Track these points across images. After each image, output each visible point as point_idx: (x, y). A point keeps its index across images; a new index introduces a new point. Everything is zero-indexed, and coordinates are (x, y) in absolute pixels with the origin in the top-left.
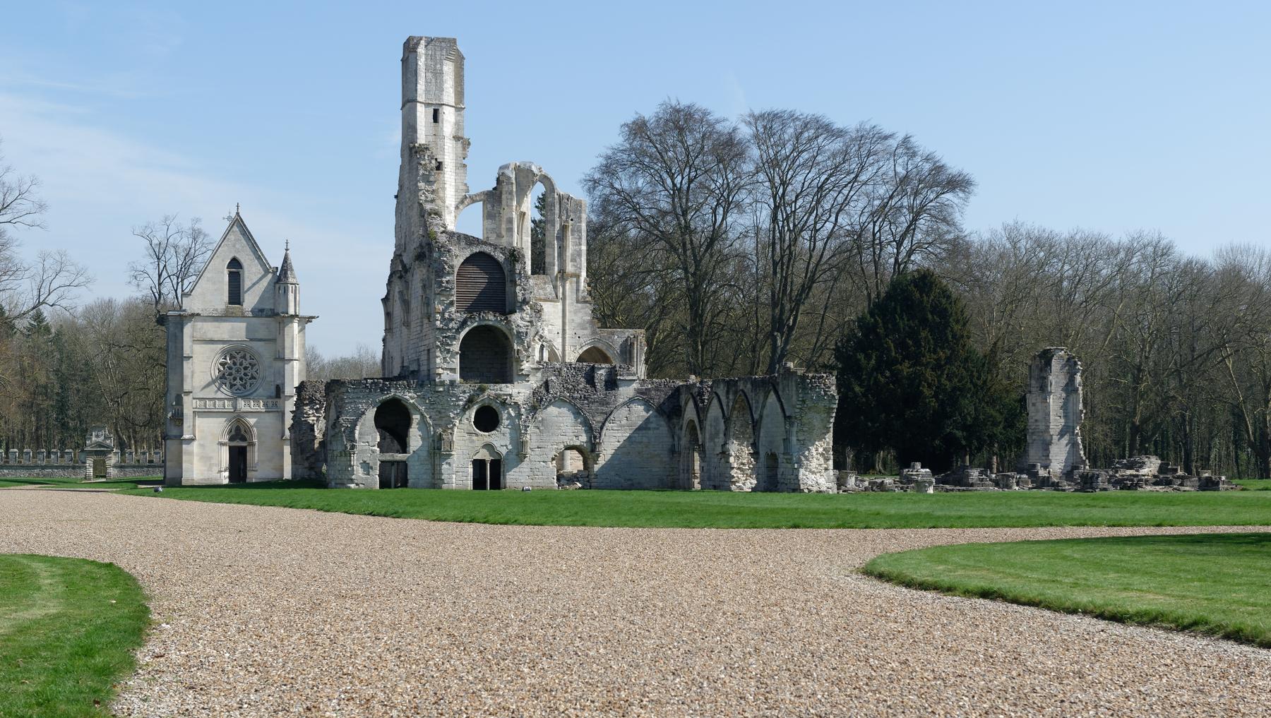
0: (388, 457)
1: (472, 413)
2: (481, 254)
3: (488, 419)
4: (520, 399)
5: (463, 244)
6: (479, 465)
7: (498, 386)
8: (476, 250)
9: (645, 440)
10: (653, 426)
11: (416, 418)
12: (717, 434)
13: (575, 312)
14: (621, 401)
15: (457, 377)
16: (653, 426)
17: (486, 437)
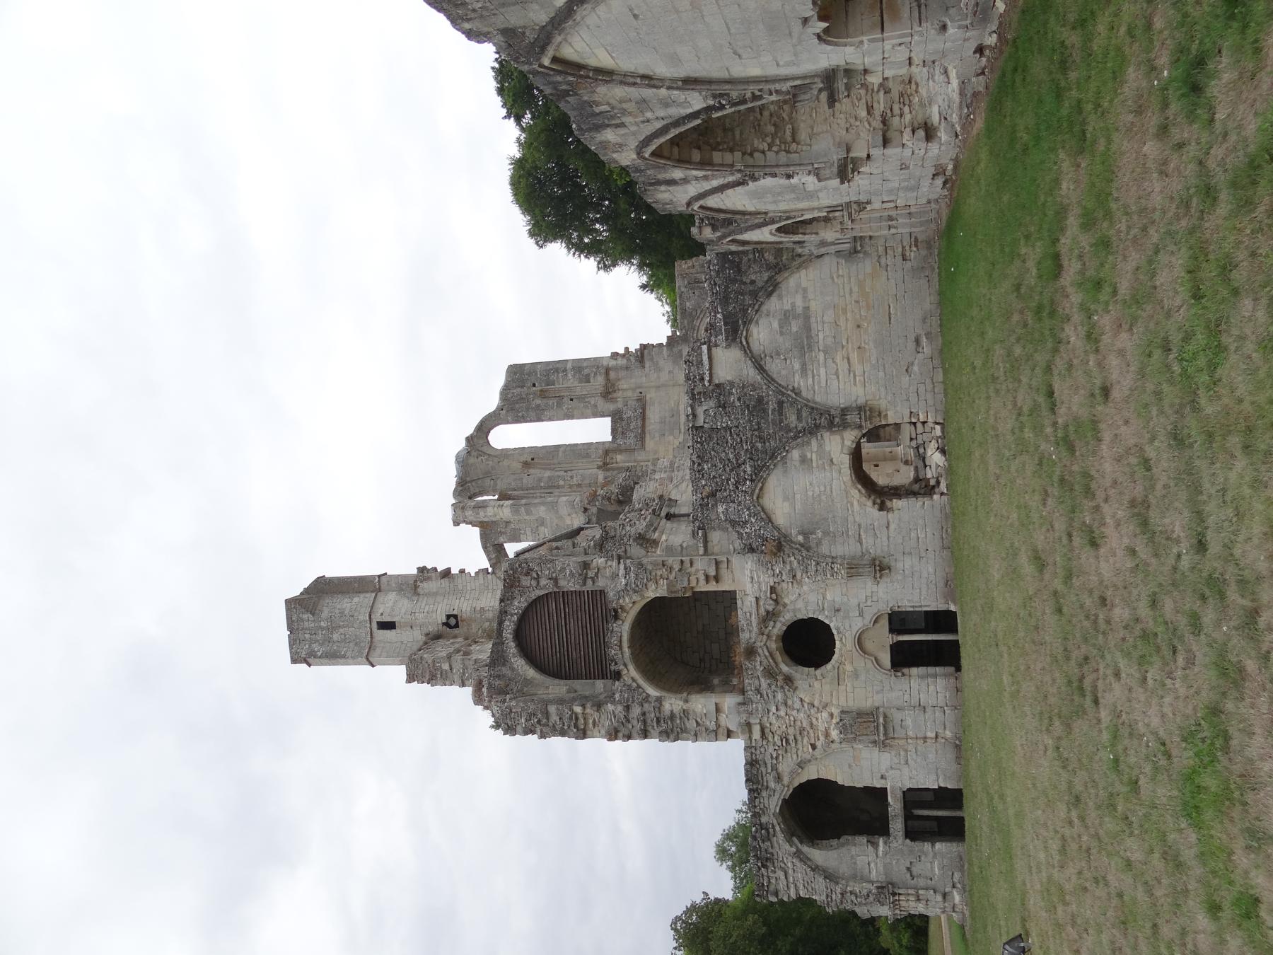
0: (897, 826)
1: (801, 674)
2: (519, 635)
3: (809, 643)
4: (767, 580)
5: (505, 670)
6: (904, 658)
7: (743, 622)
8: (512, 648)
9: (829, 316)
10: (799, 303)
11: (811, 773)
12: (793, 189)
13: (658, 369)
14: (751, 373)
15: (729, 701)
16: (799, 303)
17: (843, 645)
